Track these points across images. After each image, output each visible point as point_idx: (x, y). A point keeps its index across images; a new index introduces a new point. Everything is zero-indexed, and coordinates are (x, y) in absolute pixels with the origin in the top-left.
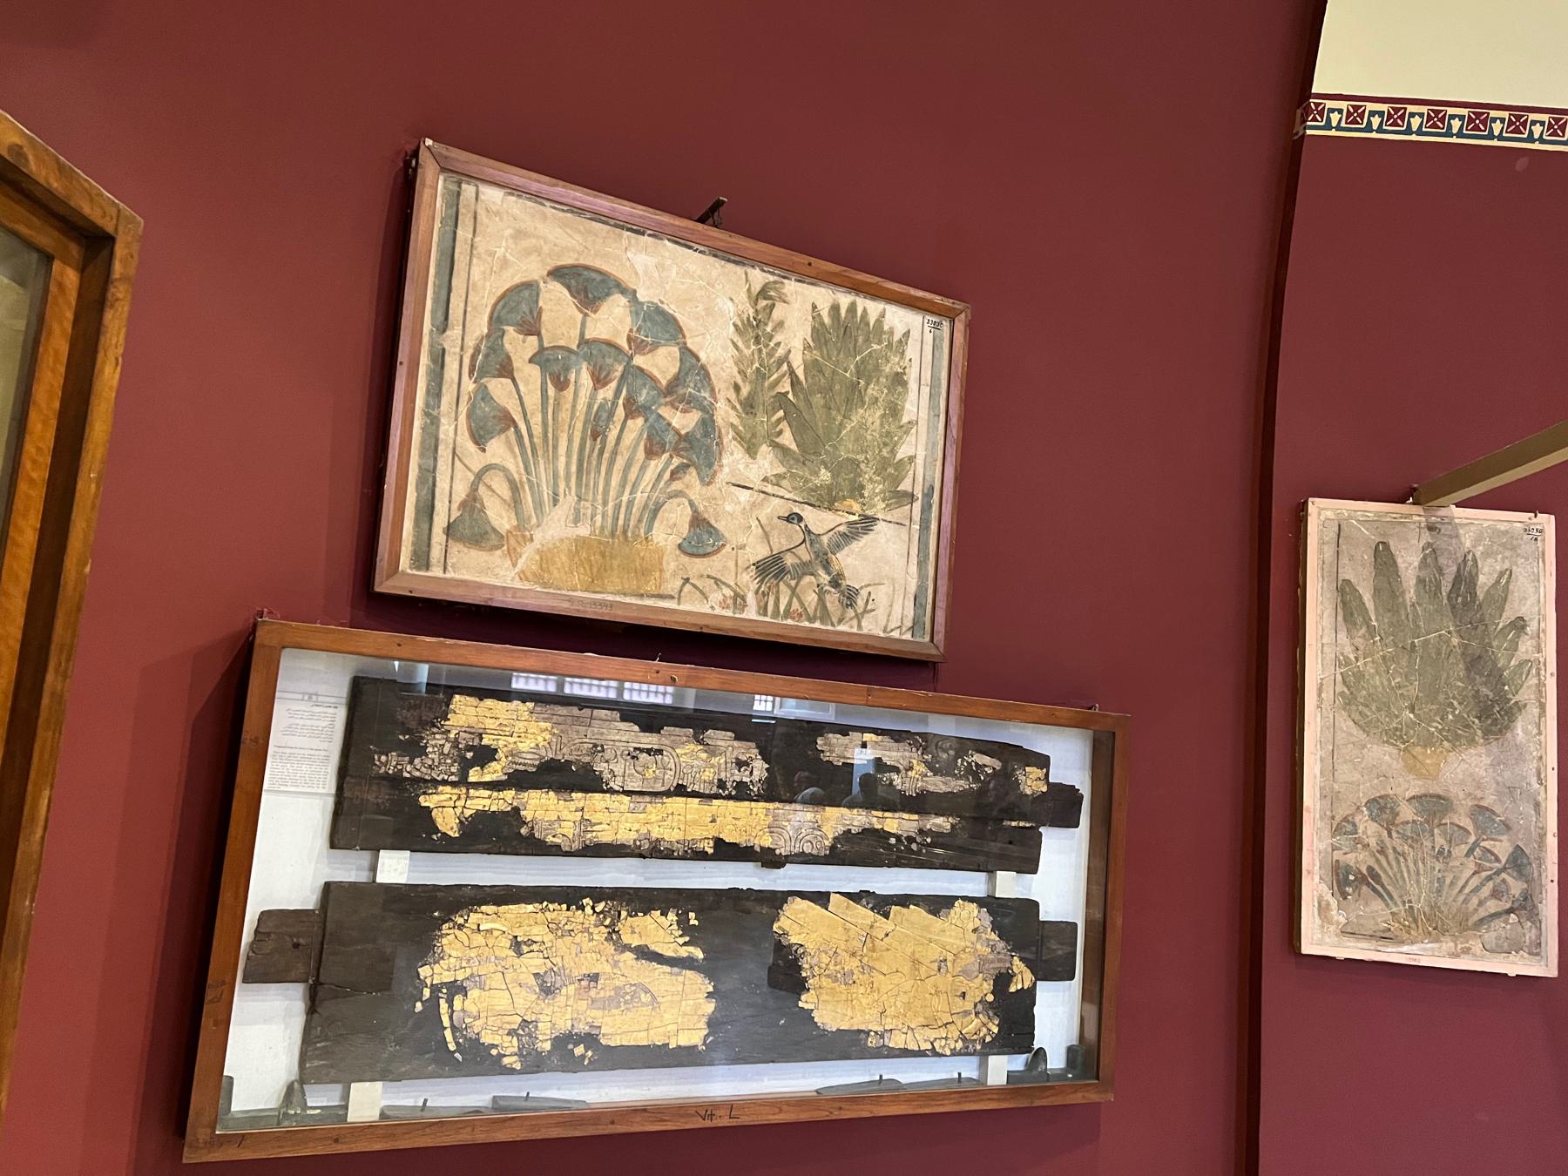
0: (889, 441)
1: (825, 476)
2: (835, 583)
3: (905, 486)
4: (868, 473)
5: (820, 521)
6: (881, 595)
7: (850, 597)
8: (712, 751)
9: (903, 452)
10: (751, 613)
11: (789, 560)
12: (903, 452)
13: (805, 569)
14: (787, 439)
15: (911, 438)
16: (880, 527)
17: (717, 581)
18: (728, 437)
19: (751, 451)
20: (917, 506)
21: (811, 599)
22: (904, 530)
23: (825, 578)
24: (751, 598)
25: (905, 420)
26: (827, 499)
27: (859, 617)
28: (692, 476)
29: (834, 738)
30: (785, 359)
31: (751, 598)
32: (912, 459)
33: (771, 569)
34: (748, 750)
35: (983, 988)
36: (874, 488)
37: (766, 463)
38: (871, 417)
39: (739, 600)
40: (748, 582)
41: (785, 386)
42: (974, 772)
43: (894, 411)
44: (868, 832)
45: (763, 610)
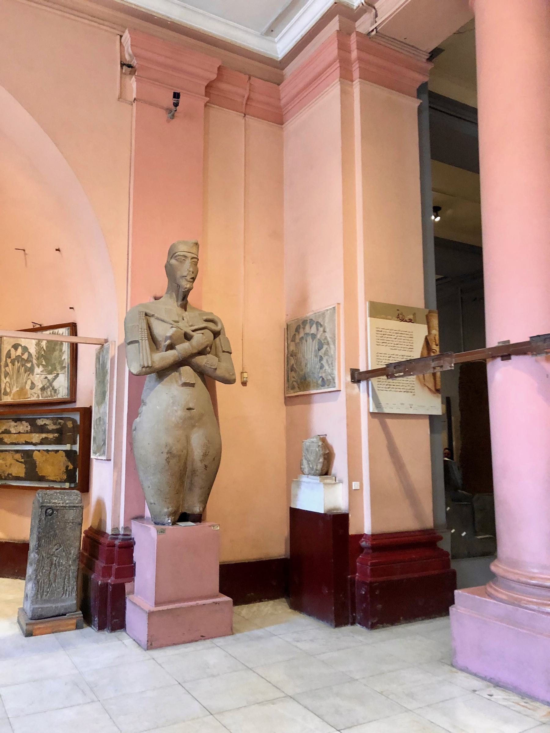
0: (60, 357)
1: (50, 368)
2: (53, 389)
3: (64, 365)
4: (57, 364)
5: (50, 377)
6: (61, 389)
7: (55, 391)
8: (23, 425)
9: (63, 358)
10: (41, 398)
11: (46, 386)
12: (63, 358)
13: (48, 387)
14: (44, 363)
15: (64, 355)
16: (60, 375)
17: (35, 393)
18: (35, 365)
19: (39, 367)
20: (66, 369)
21: (49, 393)
22: (64, 375)
23: (51, 388)
24: (40, 396)
25: (63, 351)
26: (50, 373)
27: (57, 395)
28: (31, 375)
29: (38, 420)
30: (43, 347)
31: (40, 396)
32: (65, 359)
33: (43, 389)
34: (27, 424)
35: (64, 469)
36: (58, 367)
37: (41, 368)
38: (56, 353)
39: (38, 396)
40: (39, 392)
41: (43, 353)
42: (60, 424)
43: (61, 350)
44: (46, 438)
45: (42, 397)
